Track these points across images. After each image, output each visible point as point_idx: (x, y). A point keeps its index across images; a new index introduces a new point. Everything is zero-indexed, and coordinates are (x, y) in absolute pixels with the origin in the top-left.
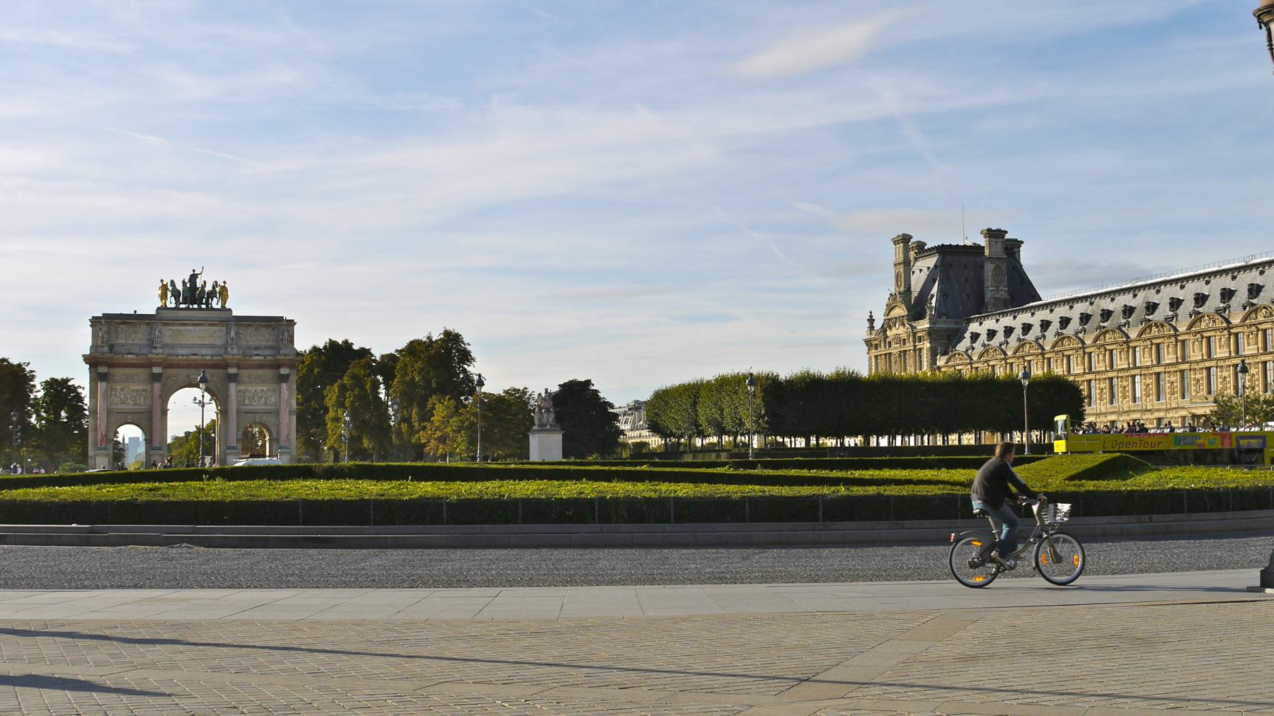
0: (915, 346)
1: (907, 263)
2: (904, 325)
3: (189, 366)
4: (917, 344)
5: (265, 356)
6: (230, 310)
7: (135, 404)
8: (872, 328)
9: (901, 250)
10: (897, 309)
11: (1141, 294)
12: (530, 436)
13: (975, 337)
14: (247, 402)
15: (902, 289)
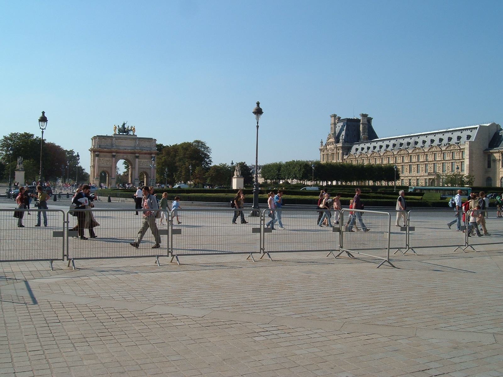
0: (337, 152)
1: (335, 124)
2: (333, 145)
3: (124, 153)
4: (337, 151)
5: (147, 150)
6: (136, 135)
7: (106, 165)
8: (322, 145)
9: (333, 119)
10: (331, 139)
11: (413, 138)
12: (233, 179)
13: (357, 149)
14: (141, 165)
15: (333, 132)
